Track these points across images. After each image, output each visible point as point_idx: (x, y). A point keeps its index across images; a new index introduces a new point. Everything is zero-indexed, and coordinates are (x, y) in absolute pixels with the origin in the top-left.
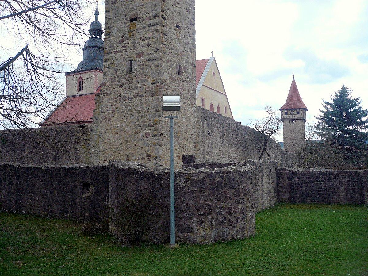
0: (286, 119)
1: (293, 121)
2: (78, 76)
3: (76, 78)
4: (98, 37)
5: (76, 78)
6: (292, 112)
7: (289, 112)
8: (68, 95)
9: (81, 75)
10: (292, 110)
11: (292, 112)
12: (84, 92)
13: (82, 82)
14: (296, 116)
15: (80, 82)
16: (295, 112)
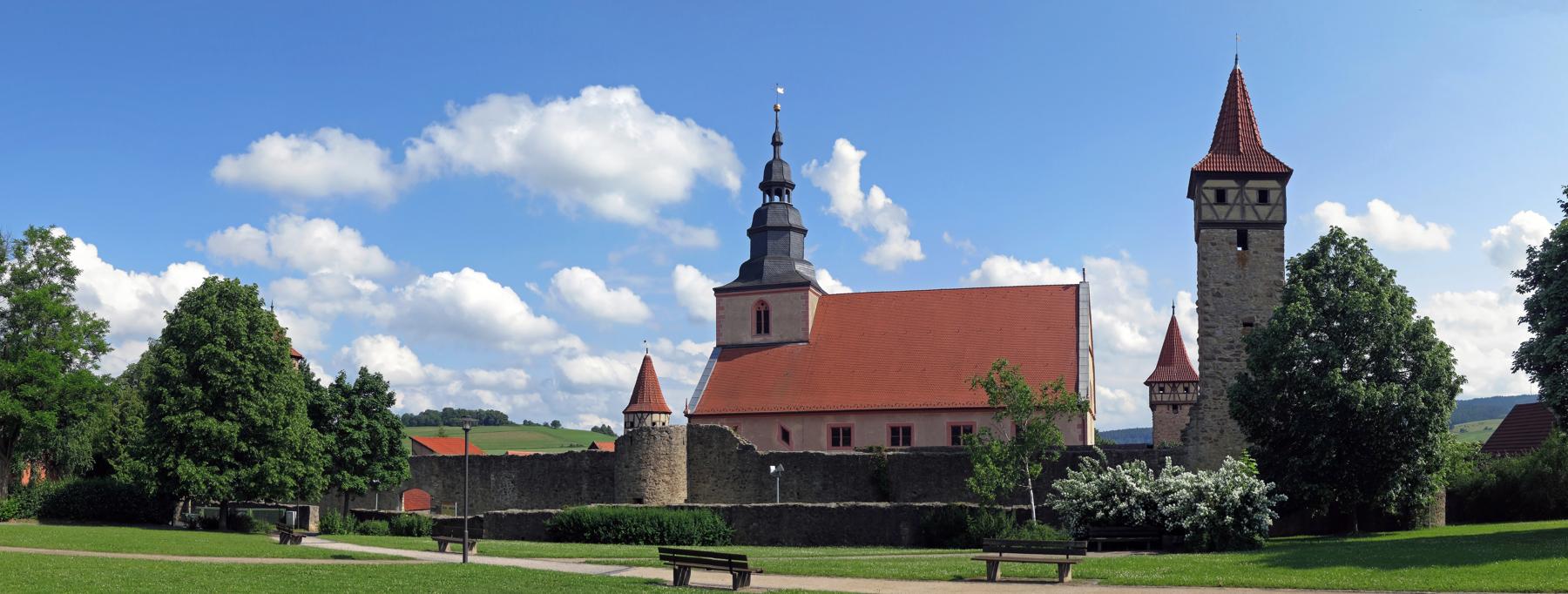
0: (1162, 403)
1: (1175, 407)
2: (756, 298)
3: (748, 302)
4: (777, 199)
5: (747, 304)
6: (1174, 388)
7: (1168, 389)
8: (724, 341)
9: (764, 297)
10: (1174, 384)
11: (1174, 388)
12: (773, 337)
13: (767, 313)
14: (1183, 397)
15: (759, 313)
16: (1180, 389)
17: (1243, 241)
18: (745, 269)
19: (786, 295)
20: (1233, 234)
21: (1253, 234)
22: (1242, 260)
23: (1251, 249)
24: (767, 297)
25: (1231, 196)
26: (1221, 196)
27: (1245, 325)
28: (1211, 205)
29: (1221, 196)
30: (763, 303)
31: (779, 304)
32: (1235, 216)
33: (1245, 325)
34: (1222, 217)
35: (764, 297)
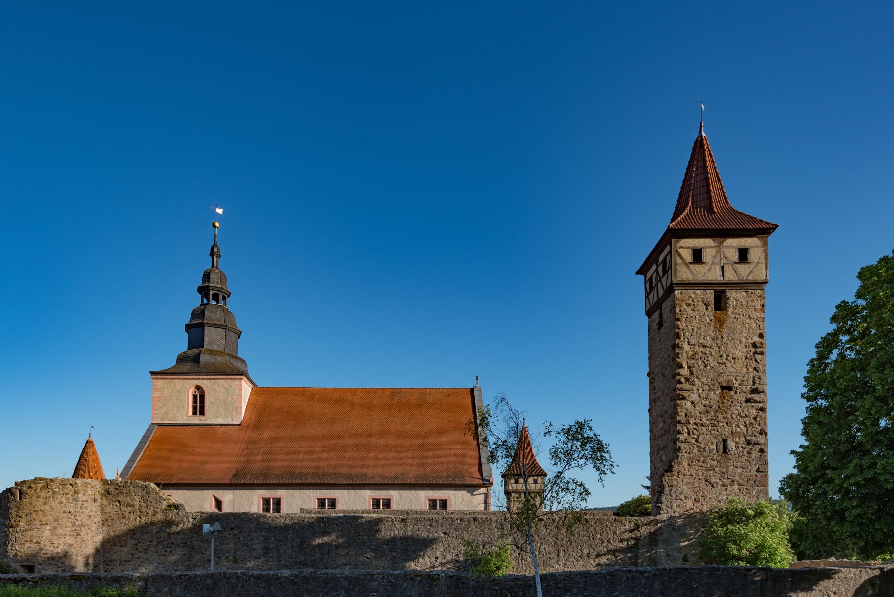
9: (198, 383)
13: (202, 397)
15: (195, 397)
17: (720, 302)
18: (181, 359)
19: (223, 381)
20: (710, 295)
21: (732, 294)
22: (720, 323)
23: (730, 311)
24: (205, 384)
25: (707, 256)
26: (697, 256)
27: (723, 388)
28: (687, 265)
29: (697, 256)
30: (198, 388)
31: (214, 388)
32: (715, 275)
33: (723, 388)
34: (700, 278)
35: (198, 383)
